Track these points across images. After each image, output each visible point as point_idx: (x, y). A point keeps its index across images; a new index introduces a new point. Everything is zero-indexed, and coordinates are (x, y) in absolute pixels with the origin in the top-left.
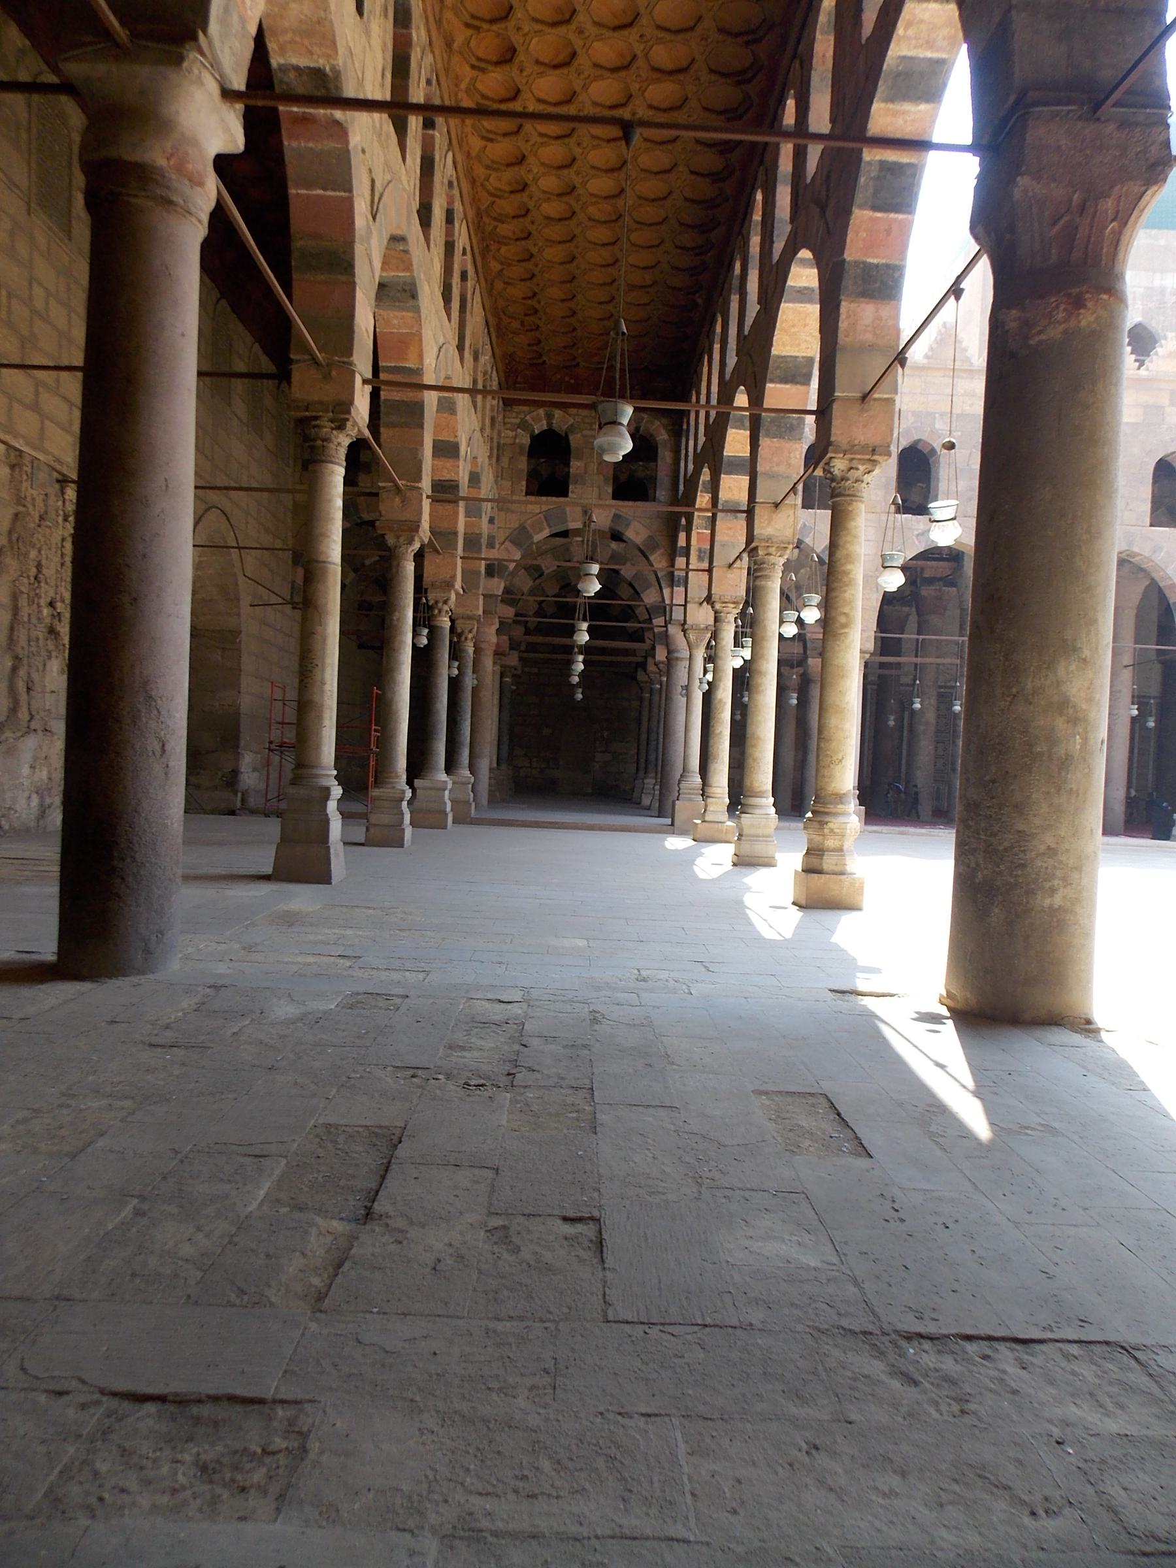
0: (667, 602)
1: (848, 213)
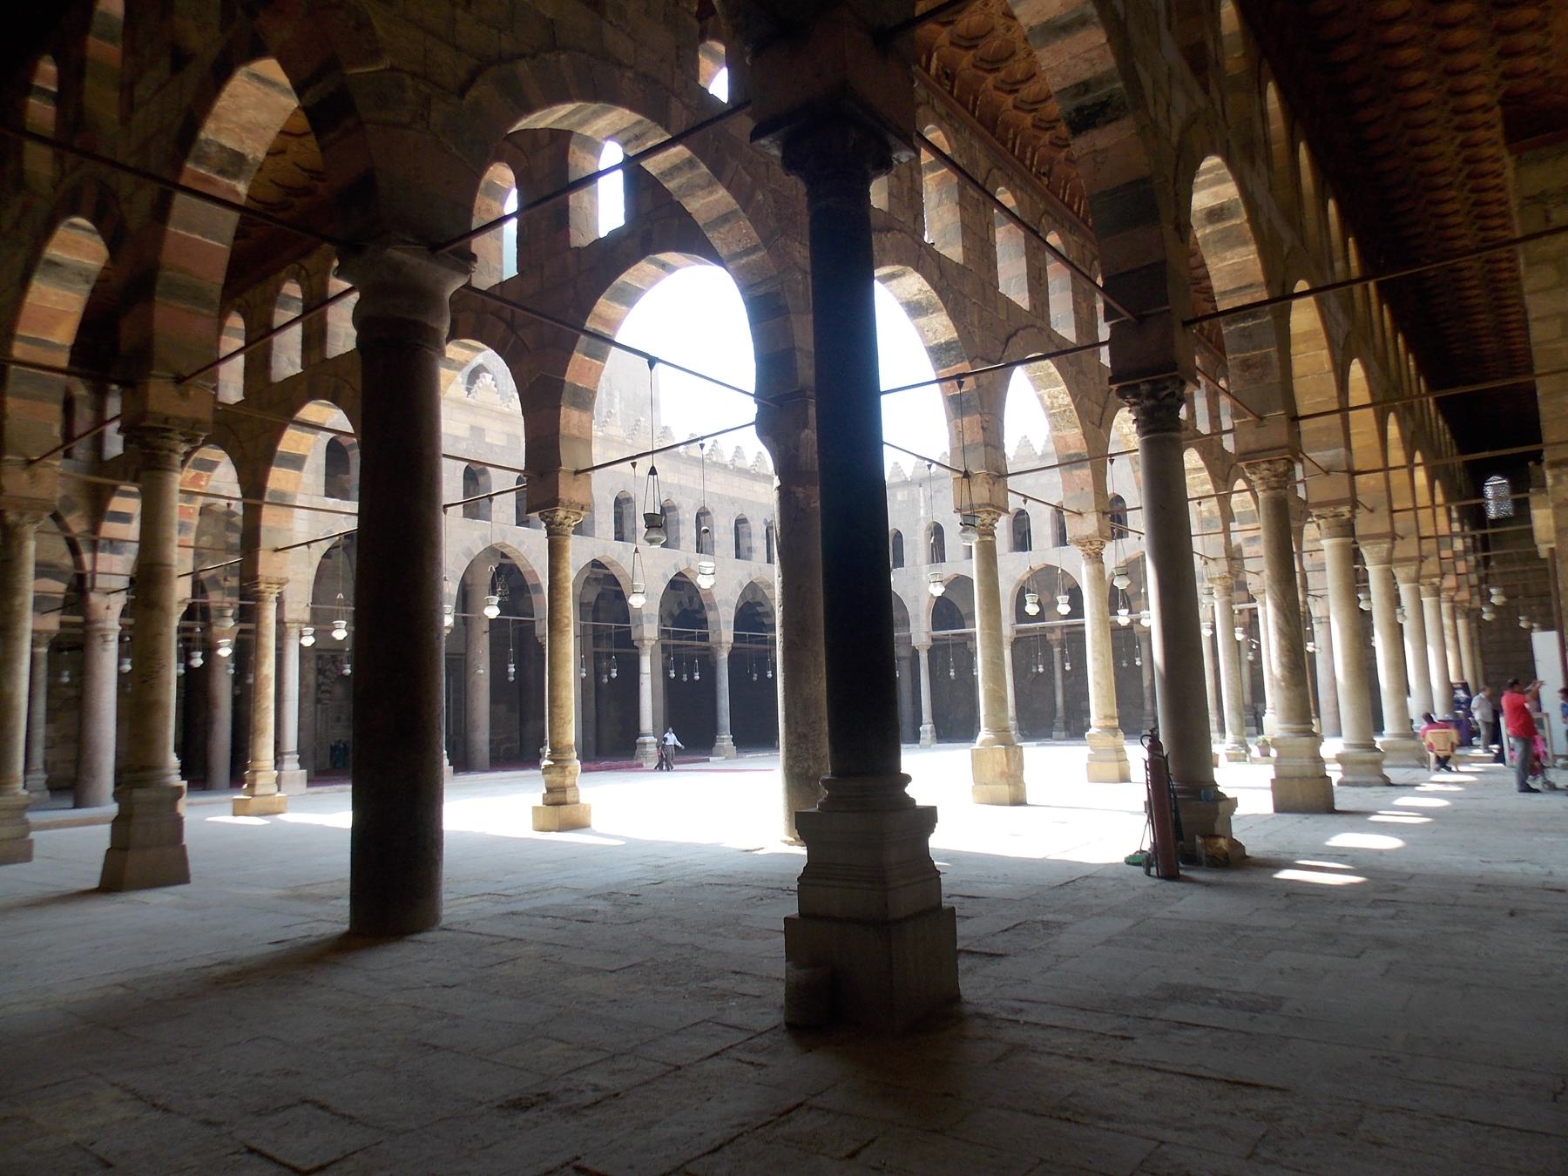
0: (88, 567)
1: (571, 353)
